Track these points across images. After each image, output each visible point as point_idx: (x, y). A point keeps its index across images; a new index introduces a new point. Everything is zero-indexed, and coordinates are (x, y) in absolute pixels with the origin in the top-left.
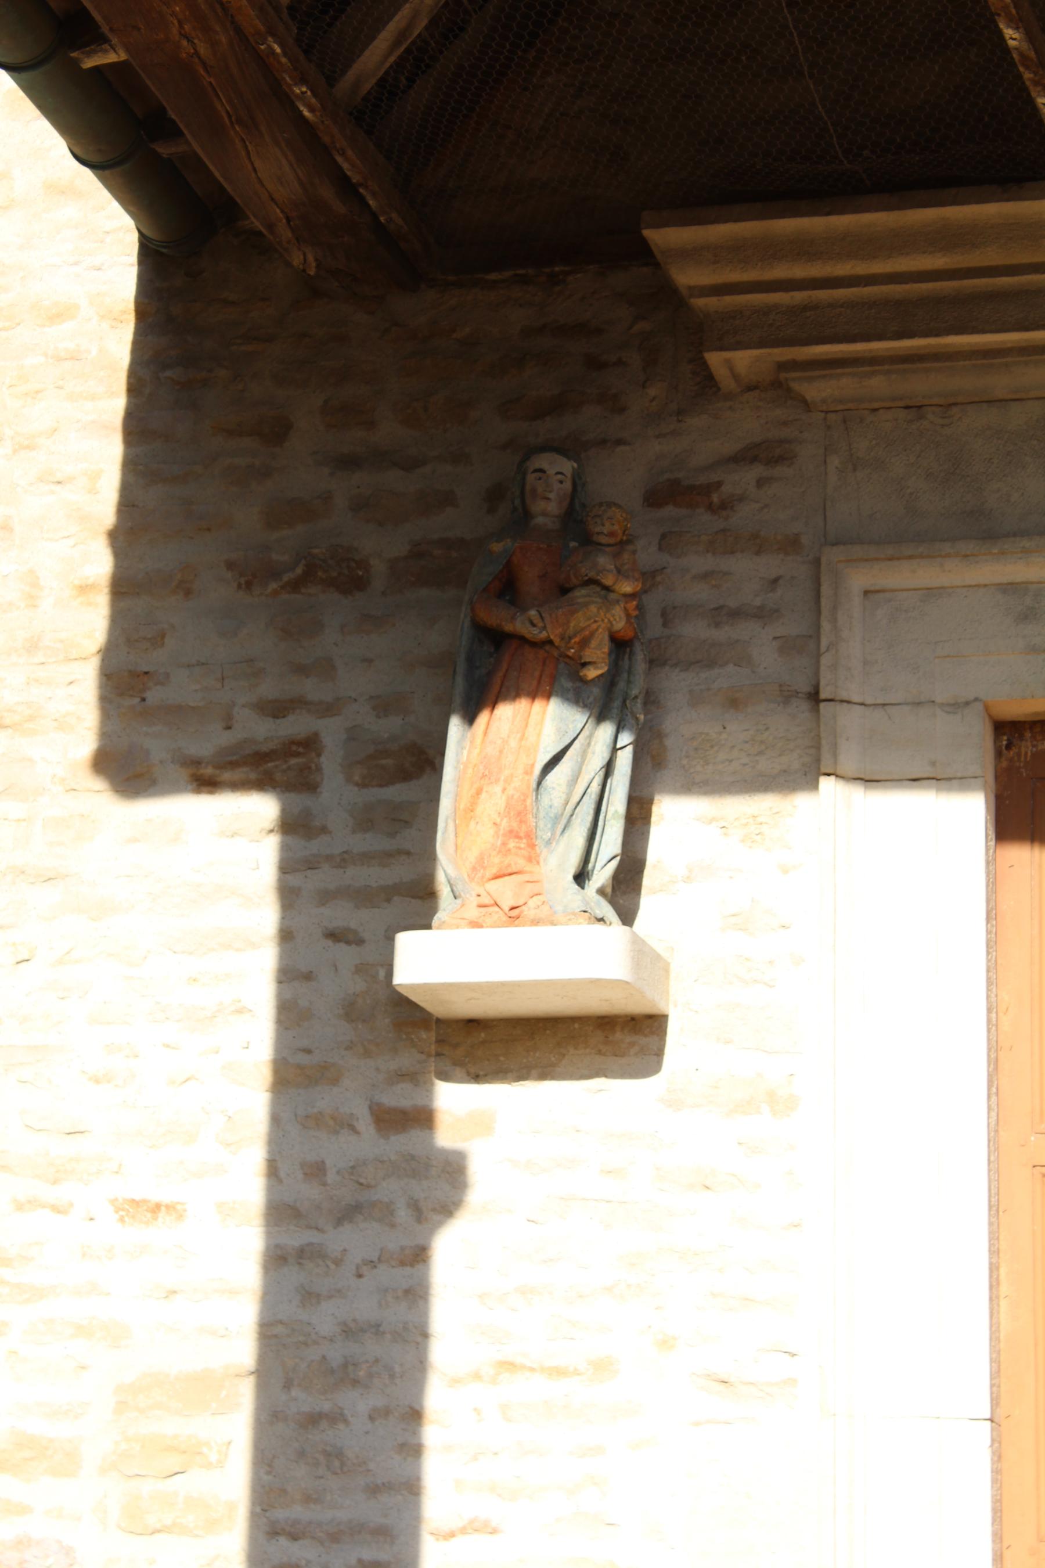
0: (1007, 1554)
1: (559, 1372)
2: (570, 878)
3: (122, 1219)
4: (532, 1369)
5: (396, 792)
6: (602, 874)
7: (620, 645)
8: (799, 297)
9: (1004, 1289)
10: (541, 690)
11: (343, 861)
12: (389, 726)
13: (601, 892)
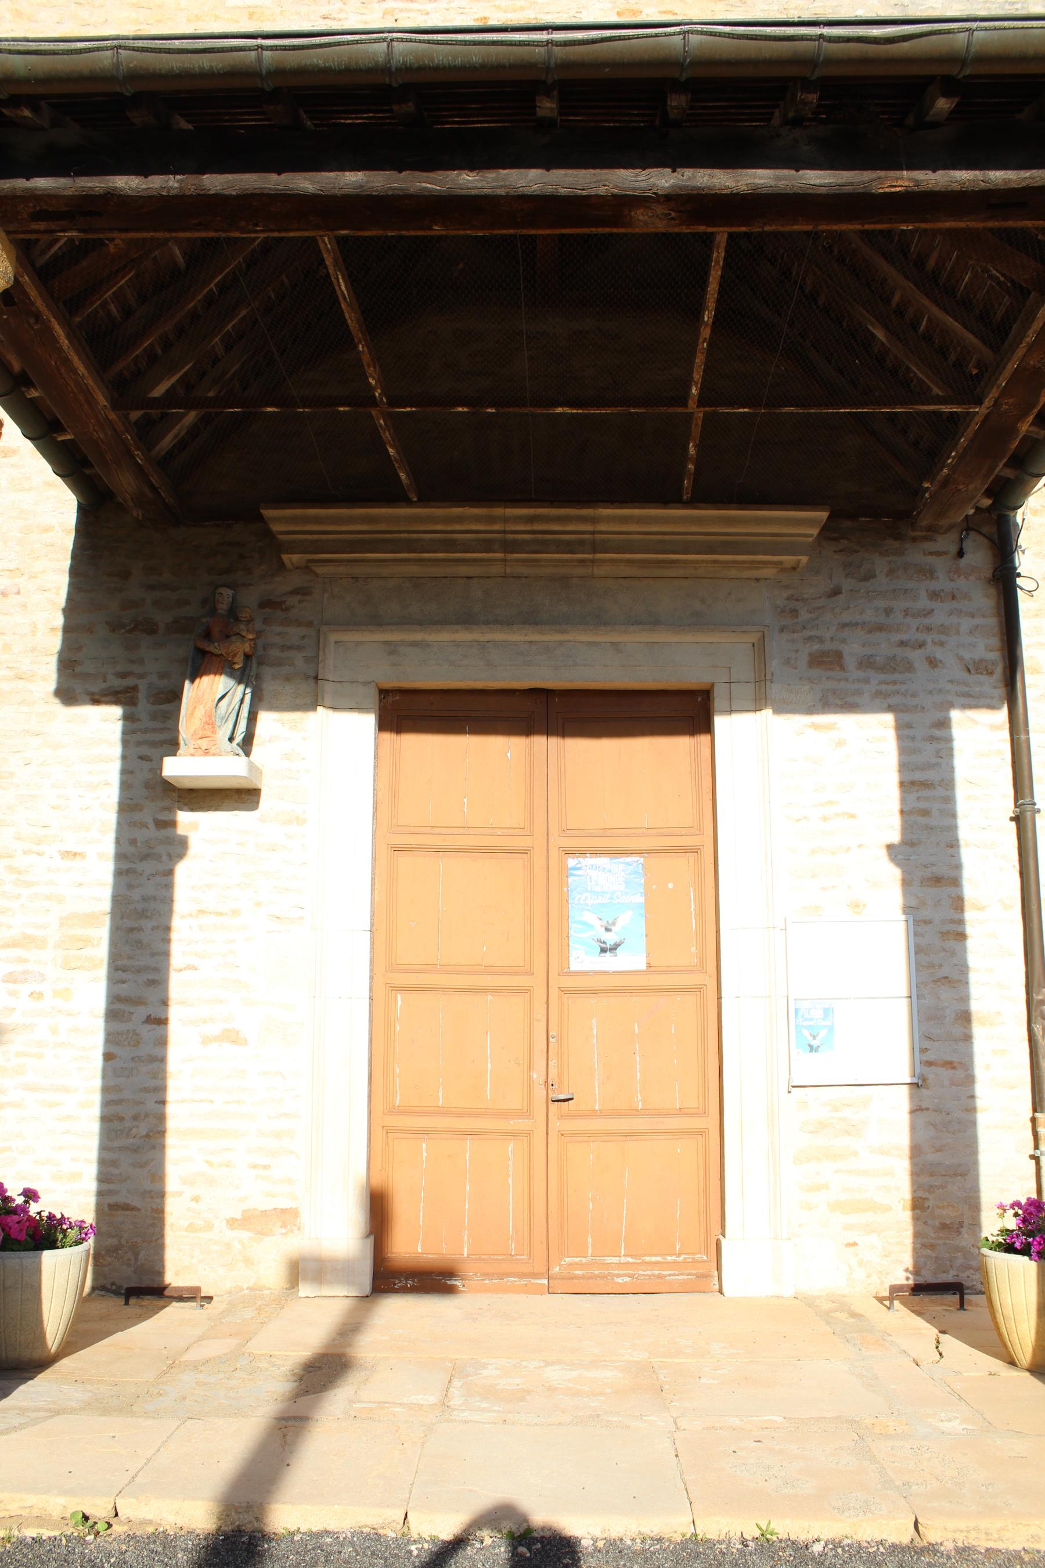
0: (375, 976)
1: (220, 914)
2: (227, 739)
3: (62, 858)
4: (210, 913)
5: (165, 707)
6: (239, 738)
7: (247, 657)
8: (315, 537)
9: (376, 886)
10: (218, 672)
11: (146, 731)
12: (163, 683)
13: (238, 745)
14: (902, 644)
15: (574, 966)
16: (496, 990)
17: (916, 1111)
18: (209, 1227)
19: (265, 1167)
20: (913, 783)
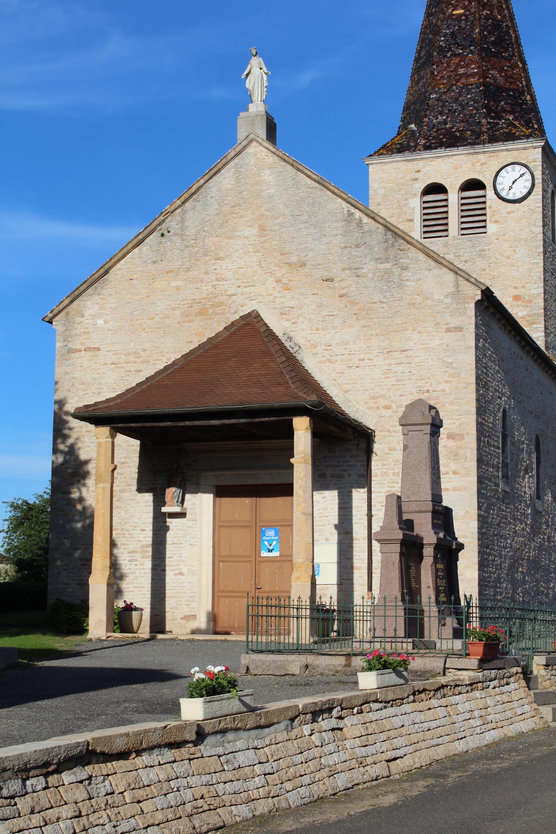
6: (180, 501)
7: (181, 481)
10: (173, 486)
14: (342, 470)
15: (262, 555)
18: (176, 619)
20: (342, 508)
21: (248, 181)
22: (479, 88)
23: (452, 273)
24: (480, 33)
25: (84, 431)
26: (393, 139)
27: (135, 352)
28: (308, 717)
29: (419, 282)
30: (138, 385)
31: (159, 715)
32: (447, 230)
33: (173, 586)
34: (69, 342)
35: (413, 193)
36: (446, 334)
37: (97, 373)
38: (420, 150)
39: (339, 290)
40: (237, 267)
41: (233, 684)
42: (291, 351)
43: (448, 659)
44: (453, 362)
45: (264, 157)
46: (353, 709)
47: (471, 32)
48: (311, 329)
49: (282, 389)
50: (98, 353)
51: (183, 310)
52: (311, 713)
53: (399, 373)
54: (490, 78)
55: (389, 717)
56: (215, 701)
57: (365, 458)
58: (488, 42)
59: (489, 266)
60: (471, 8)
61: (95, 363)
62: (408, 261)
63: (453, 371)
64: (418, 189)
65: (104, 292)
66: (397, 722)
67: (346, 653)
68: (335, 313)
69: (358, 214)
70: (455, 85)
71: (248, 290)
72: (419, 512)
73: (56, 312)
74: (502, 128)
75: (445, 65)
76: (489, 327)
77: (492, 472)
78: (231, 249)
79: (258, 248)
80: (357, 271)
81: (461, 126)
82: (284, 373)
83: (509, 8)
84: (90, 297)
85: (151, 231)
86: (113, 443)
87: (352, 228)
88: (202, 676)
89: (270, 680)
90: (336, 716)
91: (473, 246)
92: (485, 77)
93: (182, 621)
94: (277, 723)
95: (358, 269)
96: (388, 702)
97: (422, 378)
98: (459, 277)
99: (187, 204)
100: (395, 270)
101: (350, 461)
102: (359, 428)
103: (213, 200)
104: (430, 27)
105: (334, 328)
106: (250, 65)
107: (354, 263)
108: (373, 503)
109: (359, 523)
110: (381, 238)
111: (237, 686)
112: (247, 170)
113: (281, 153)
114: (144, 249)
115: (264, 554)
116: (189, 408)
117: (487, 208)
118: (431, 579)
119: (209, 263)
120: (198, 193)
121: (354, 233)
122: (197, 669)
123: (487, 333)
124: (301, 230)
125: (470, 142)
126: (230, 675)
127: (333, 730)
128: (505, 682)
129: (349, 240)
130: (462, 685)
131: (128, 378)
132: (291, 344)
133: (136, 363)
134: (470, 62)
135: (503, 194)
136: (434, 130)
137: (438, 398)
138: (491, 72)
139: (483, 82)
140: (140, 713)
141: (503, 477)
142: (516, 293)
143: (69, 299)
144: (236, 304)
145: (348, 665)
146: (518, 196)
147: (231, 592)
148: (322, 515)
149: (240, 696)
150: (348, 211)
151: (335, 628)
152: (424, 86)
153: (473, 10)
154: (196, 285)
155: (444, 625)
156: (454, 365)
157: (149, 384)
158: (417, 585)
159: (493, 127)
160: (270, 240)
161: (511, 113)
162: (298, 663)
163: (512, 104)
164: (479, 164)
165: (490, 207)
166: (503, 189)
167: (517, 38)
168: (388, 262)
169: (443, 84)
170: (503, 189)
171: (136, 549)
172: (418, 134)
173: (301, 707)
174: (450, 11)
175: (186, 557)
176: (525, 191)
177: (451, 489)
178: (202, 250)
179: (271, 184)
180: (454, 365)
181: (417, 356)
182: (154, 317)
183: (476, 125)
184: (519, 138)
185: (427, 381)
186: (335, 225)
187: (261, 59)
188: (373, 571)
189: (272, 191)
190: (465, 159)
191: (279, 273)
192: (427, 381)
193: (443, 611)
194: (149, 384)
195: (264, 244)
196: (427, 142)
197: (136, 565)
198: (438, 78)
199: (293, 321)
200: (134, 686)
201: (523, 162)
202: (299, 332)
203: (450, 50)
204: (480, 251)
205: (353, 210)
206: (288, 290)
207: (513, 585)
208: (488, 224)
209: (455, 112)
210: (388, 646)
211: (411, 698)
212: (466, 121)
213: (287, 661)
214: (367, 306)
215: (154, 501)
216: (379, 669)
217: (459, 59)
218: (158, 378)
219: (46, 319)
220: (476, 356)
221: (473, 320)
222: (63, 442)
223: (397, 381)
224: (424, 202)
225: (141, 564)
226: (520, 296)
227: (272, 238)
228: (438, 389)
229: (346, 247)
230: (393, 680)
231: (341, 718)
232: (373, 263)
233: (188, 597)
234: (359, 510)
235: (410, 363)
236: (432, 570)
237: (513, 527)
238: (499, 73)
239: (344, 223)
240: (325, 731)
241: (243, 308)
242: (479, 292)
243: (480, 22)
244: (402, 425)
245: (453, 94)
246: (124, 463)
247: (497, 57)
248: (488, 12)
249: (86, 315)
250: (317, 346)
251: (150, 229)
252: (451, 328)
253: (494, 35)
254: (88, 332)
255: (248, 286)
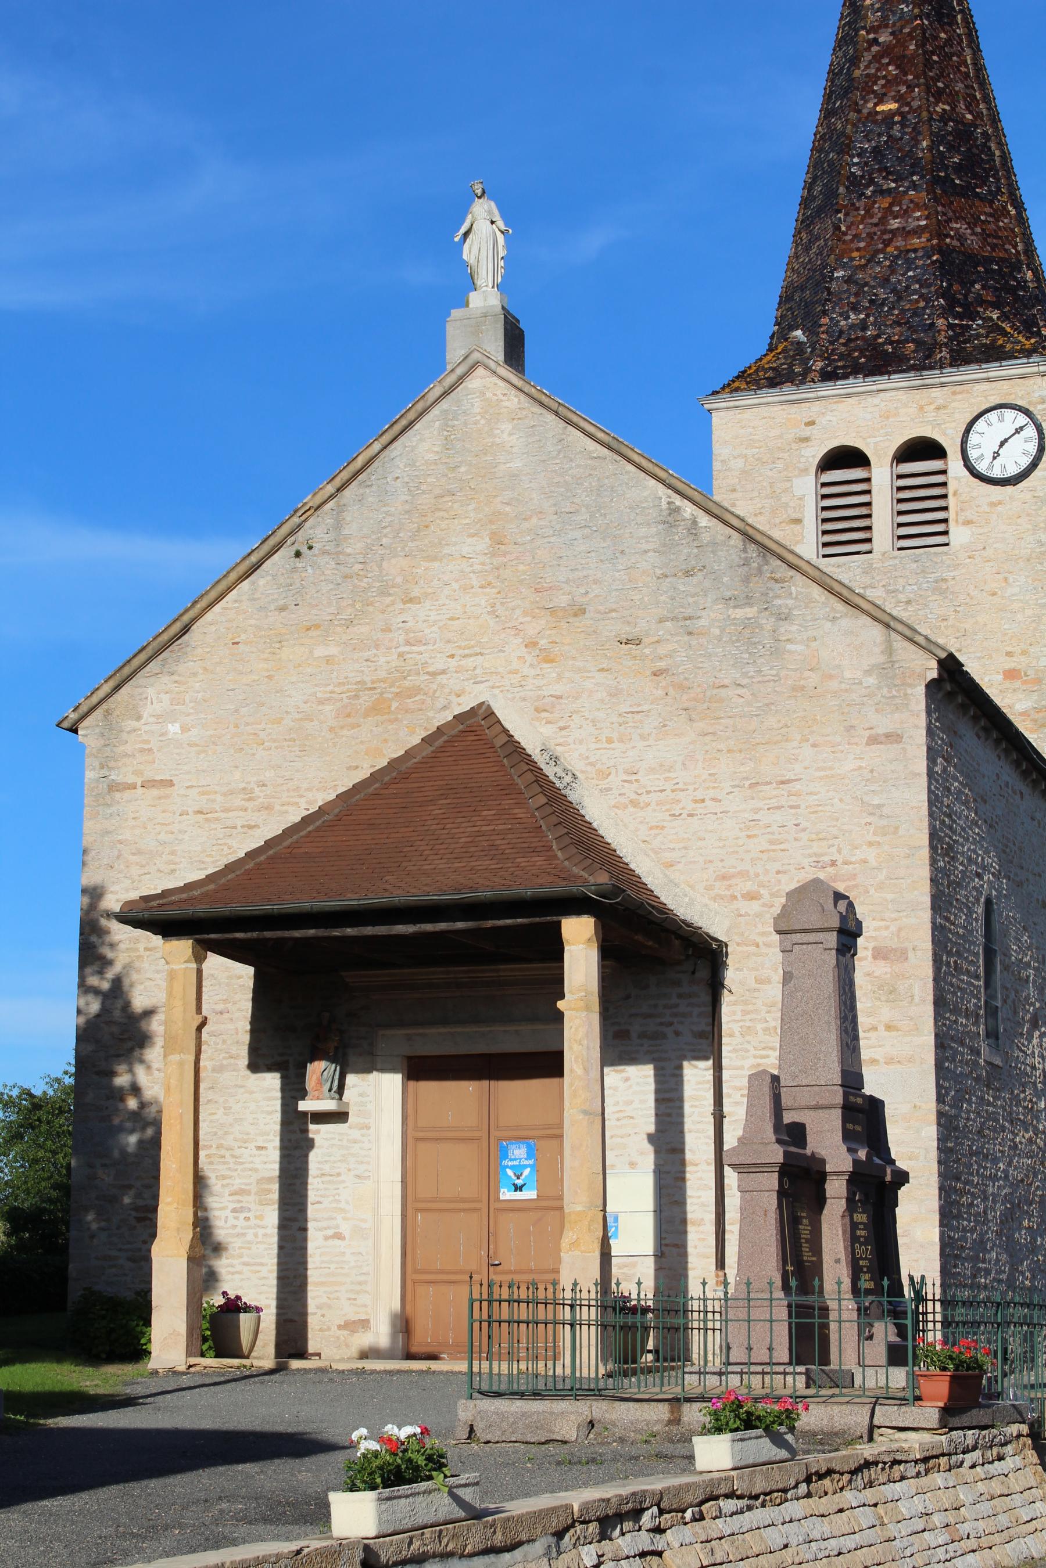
6: (335, 1088)
7: (337, 1048)
10: (321, 1059)
14: (661, 1024)
15: (502, 1197)
16: (464, 1210)
17: (657, 1270)
18: (329, 1329)
19: (355, 1299)
20: (663, 1099)
21: (467, 446)
22: (929, 257)
23: (880, 626)
24: (930, 148)
25: (142, 949)
26: (760, 359)
27: (244, 789)
28: (590, 1530)
29: (814, 644)
30: (250, 855)
31: (290, 1527)
32: (869, 540)
33: (323, 1262)
34: (110, 769)
35: (801, 466)
36: (868, 748)
37: (167, 832)
38: (813, 381)
39: (652, 661)
40: (448, 616)
41: (437, 1462)
42: (558, 784)
43: (877, 1408)
44: (884, 805)
45: (501, 397)
46: (684, 1511)
47: (913, 147)
48: (598, 740)
49: (539, 861)
50: (168, 791)
51: (339, 704)
52: (599, 1520)
53: (774, 828)
54: (952, 238)
55: (759, 1528)
56: (400, 1497)
57: (708, 999)
58: (947, 167)
59: (955, 611)
60: (913, 99)
61: (164, 812)
62: (790, 602)
63: (884, 822)
64: (811, 459)
65: (181, 668)
66: (774, 1537)
67: (670, 1396)
68: (645, 708)
69: (688, 509)
70: (883, 251)
71: (469, 662)
72: (816, 1108)
73: (84, 709)
74: (978, 336)
75: (862, 212)
76: (955, 733)
77: (966, 1026)
78: (436, 582)
79: (490, 578)
80: (688, 622)
81: (896, 333)
82: (544, 828)
83: (987, 99)
84: (152, 679)
85: (274, 547)
86: (199, 972)
87: (677, 538)
88: (374, 1446)
89: (516, 1452)
90: (649, 1526)
91: (923, 571)
92: (942, 236)
93: (339, 1332)
94: (529, 1541)
95: (690, 618)
96: (756, 1497)
97: (820, 836)
98: (893, 634)
99: (347, 493)
100: (764, 621)
101: (677, 1006)
102: (694, 939)
103: (399, 483)
104: (830, 138)
105: (643, 737)
106: (469, 217)
107: (682, 607)
108: (725, 1090)
109: (698, 1131)
110: (735, 557)
111: (446, 1466)
112: (465, 424)
113: (533, 390)
114: (262, 582)
115: (507, 1194)
116: (351, 900)
117: (950, 496)
118: (842, 1243)
119: (390, 609)
120: (369, 470)
121: (681, 547)
122: (363, 1431)
123: (951, 746)
124: (575, 542)
125: (915, 365)
126: (432, 1442)
127: (643, 1555)
128: (995, 1454)
129: (671, 560)
130: (906, 1462)
131: (229, 841)
132: (558, 770)
133: (246, 810)
134: (911, 205)
135: (982, 467)
136: (842, 341)
137: (854, 876)
138: (955, 225)
139: (937, 244)
140: (250, 1523)
141: (988, 1035)
142: (1009, 664)
143: (112, 684)
144: (447, 690)
145: (675, 1421)
146: (1012, 471)
147: (441, 1272)
148: (621, 1115)
149: (451, 1488)
150: (669, 503)
151: (650, 1346)
152: (821, 253)
153: (916, 104)
154: (366, 654)
155: (870, 1337)
156: (885, 811)
157: (271, 852)
158: (813, 1256)
159: (960, 333)
160: (513, 563)
161: (996, 305)
162: (573, 1417)
163: (996, 289)
164: (932, 407)
165: (955, 494)
166: (981, 457)
167: (1006, 158)
168: (751, 605)
169: (858, 249)
170: (981, 457)
171: (248, 1187)
172: (809, 350)
173: (576, 1508)
174: (870, 105)
175: (347, 1203)
176: (1025, 462)
177: (881, 1060)
178: (378, 584)
179: (514, 450)
180: (885, 811)
181: (811, 794)
182: (282, 719)
183: (925, 331)
184: (1012, 357)
185: (831, 842)
186: (643, 531)
187: (493, 204)
188: (727, 1227)
189: (517, 464)
190: (904, 397)
191: (532, 630)
192: (831, 842)
193: (866, 1309)
194: (271, 852)
195: (501, 571)
196: (827, 366)
197: (247, 1219)
198: (849, 237)
199: (561, 724)
200: (240, 1467)
201: (1020, 403)
202: (572, 746)
203: (871, 181)
204: (936, 582)
205: (678, 501)
206: (552, 661)
207: (1011, 1256)
208: (952, 527)
209: (883, 304)
210: (756, 1381)
211: (803, 1488)
212: (905, 324)
213: (552, 1413)
214: (708, 694)
215: (283, 1090)
216: (737, 1430)
217: (889, 200)
218: (290, 840)
219: (66, 724)
220: (930, 791)
221: (922, 720)
222: (101, 973)
223: (771, 842)
224: (824, 485)
225: (256, 1217)
226: (1019, 671)
227: (517, 558)
228: (853, 859)
229: (666, 576)
230: (765, 1450)
231: (658, 1530)
232: (720, 606)
233: (352, 1283)
234: (697, 1103)
235: (798, 807)
236: (843, 1225)
237: (1010, 1136)
238: (971, 226)
239: (661, 527)
240: (628, 1557)
241: (461, 700)
242: (934, 664)
243: (931, 126)
244: (779, 932)
245: (878, 269)
246: (221, 1013)
247: (964, 195)
248: (947, 108)
249: (145, 716)
250: (610, 774)
251: (272, 542)
252: (878, 735)
253: (958, 152)
254: (150, 750)
255: (471, 655)
